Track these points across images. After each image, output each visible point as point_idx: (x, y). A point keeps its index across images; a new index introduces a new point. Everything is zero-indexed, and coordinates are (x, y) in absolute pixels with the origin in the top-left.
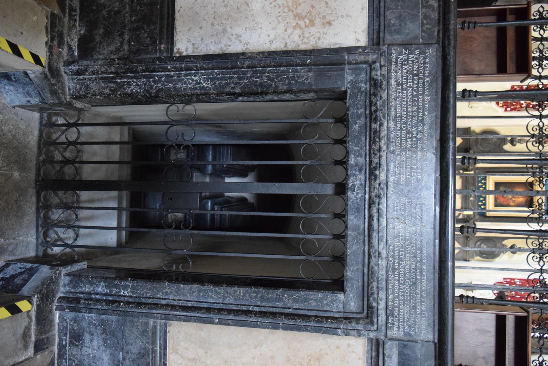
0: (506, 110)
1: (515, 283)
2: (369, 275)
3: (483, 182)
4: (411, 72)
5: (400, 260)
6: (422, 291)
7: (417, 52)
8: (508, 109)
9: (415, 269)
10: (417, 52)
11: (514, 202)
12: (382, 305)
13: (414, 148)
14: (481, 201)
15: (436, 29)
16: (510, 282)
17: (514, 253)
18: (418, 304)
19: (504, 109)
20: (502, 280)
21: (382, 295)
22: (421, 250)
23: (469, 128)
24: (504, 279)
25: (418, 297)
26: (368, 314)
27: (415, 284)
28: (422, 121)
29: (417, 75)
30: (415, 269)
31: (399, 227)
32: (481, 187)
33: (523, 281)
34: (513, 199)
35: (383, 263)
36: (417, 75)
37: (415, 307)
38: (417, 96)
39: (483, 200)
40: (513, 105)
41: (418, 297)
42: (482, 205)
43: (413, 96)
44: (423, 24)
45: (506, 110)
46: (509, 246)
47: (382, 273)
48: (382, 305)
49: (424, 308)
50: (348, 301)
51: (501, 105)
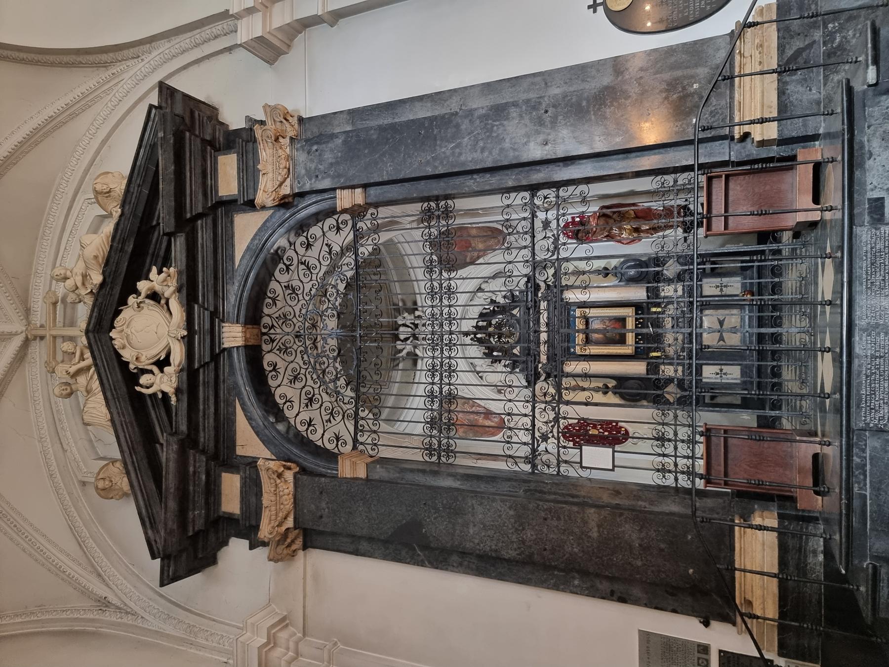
4: (876, 411)
5: (884, 280)
6: (866, 260)
7: (871, 425)
9: (872, 274)
10: (871, 425)
13: (874, 357)
14: (640, 323)
15: (855, 440)
17: (606, 269)
18: (869, 250)
22: (867, 288)
25: (869, 255)
27: (872, 264)
28: (867, 376)
29: (872, 409)
30: (872, 274)
32: (640, 340)
36: (872, 409)
37: (872, 248)
38: (871, 394)
41: (869, 255)
43: (875, 394)
44: (866, 445)
49: (865, 248)
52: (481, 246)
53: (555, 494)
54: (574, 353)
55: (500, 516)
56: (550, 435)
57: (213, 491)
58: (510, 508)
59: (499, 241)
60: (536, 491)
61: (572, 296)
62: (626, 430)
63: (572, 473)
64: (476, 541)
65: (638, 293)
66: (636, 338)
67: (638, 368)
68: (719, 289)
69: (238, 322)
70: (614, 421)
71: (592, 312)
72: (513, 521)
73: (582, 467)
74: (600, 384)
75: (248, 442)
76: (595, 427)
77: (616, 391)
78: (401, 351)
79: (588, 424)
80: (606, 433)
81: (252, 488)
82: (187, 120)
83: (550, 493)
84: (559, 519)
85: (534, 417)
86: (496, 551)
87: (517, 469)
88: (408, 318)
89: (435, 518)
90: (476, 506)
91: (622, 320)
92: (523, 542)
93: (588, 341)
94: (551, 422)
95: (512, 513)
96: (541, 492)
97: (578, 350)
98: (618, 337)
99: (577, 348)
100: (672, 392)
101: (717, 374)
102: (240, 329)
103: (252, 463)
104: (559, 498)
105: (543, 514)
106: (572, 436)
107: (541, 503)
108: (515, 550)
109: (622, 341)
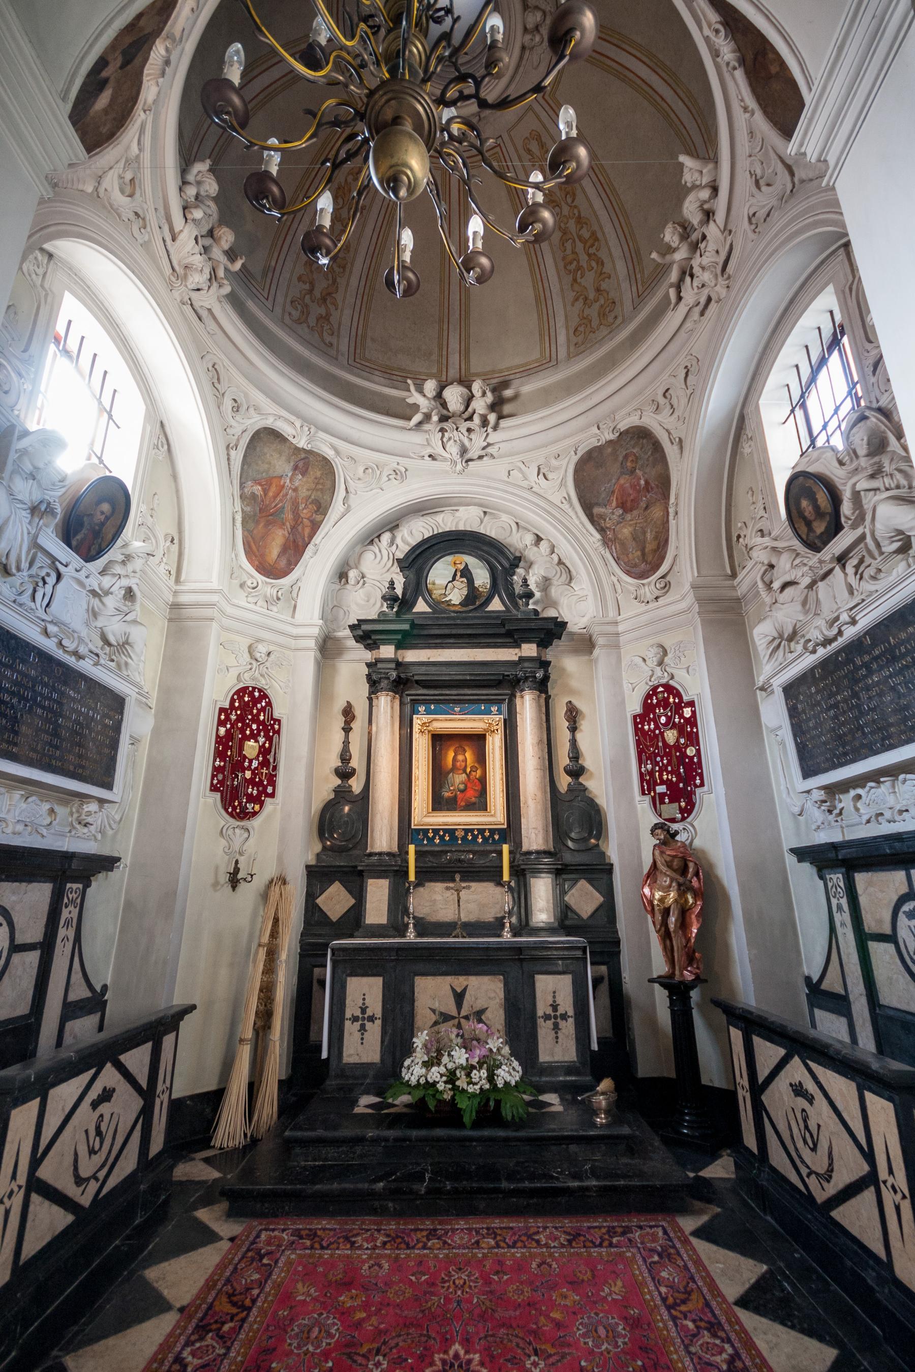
0: (272, 795)
1: (651, 773)
3: (431, 835)
8: (270, 790)
11: (474, 769)
14: (475, 837)
16: (648, 782)
19: (268, 800)
20: (647, 798)
23: (308, 867)
24: (643, 794)
32: (442, 838)
33: (644, 757)
34: (468, 770)
39: (473, 835)
40: (261, 781)
42: (483, 837)
45: (272, 795)
46: (569, 779)
51: (257, 807)
52: (626, 532)
54: (414, 712)
59: (636, 566)
61: (527, 705)
62: (255, 814)
65: (535, 834)
66: (445, 831)
67: (383, 836)
68: (549, 1011)
71: (495, 745)
74: (357, 762)
76: (264, 752)
77: (341, 794)
78: (420, 390)
79: (269, 739)
80: (248, 774)
88: (480, 405)
91: (480, 804)
93: (439, 740)
97: (417, 721)
98: (447, 795)
99: (426, 718)
100: (335, 900)
101: (363, 1011)
106: (245, 707)
109: (439, 803)
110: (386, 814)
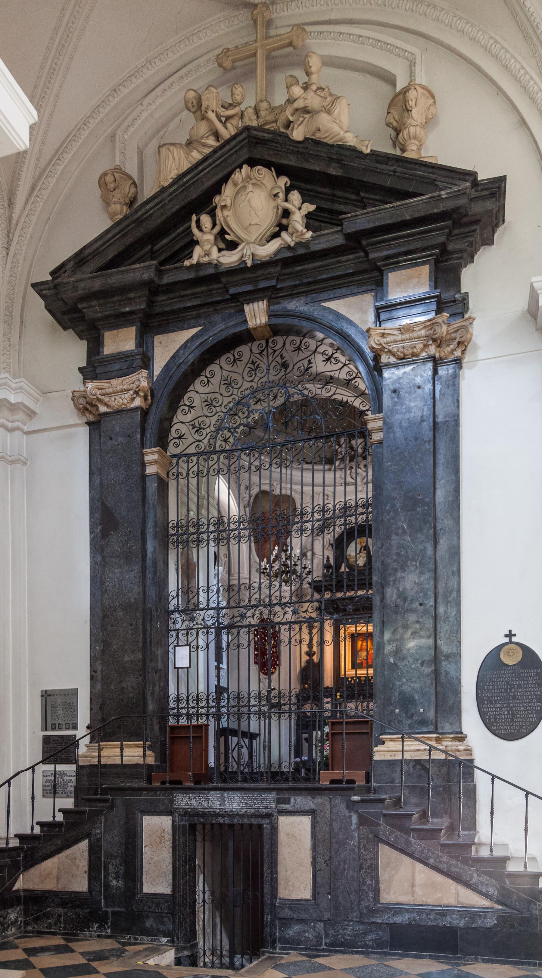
2: (254, 816)
12: (264, 810)
21: (260, 810)
26: (269, 816)
31: (235, 804)
35: (249, 810)
40: (274, 659)
47: (252, 811)
48: (264, 810)
50: (265, 822)
53: (151, 630)
55: (129, 592)
56: (195, 623)
57: (119, 320)
58: (135, 599)
60: (151, 616)
63: (171, 640)
64: (110, 575)
69: (270, 316)
70: (280, 663)
72: (127, 601)
73: (175, 647)
75: (167, 347)
81: (128, 364)
82: (465, 220)
83: (151, 626)
84: (132, 634)
85: (208, 609)
86: (106, 591)
87: (170, 598)
89: (121, 541)
90: (133, 573)
92: (115, 610)
94: (204, 622)
95: (132, 600)
96: (151, 620)
102: (264, 321)
103: (146, 362)
104: (148, 633)
105: (134, 623)
107: (141, 621)
108: (109, 605)
110: (329, 671)
